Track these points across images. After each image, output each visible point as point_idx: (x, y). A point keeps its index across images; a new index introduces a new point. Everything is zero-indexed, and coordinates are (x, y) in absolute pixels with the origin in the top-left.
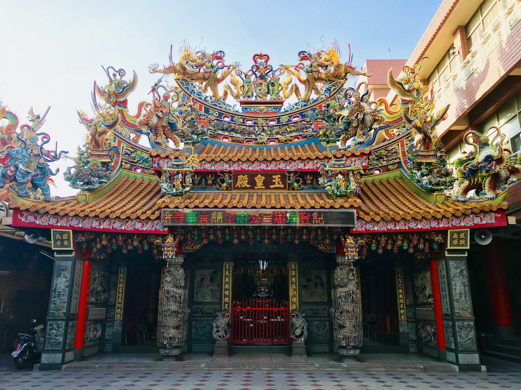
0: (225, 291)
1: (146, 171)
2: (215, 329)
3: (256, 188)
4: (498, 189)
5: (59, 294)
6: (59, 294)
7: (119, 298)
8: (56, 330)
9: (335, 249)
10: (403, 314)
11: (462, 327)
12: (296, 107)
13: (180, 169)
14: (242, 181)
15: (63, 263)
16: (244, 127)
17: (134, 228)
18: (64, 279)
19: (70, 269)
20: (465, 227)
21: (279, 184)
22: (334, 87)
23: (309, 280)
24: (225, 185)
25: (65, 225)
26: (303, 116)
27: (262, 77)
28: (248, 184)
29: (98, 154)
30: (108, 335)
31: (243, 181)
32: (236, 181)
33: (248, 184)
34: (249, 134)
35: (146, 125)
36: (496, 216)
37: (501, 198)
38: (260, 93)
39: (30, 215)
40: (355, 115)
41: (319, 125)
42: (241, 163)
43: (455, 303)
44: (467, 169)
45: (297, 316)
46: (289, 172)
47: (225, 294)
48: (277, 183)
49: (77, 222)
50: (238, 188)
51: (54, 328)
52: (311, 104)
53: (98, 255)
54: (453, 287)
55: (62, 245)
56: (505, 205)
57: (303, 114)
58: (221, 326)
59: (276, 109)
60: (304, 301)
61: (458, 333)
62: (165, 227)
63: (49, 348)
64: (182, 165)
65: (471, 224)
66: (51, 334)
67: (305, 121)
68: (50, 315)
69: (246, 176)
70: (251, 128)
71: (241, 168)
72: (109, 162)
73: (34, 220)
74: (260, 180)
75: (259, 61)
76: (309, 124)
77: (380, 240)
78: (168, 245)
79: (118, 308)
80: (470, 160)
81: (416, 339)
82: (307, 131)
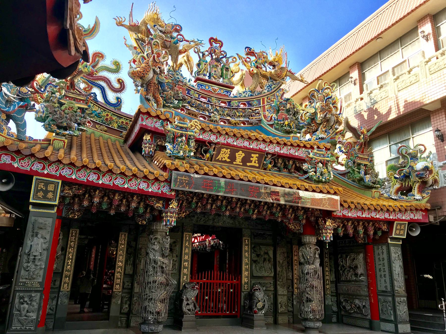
0: (184, 263)
1: (97, 126)
2: (185, 303)
3: (234, 163)
4: (424, 193)
5: (34, 259)
6: (34, 259)
7: (68, 265)
8: (27, 304)
9: (302, 229)
10: (328, 289)
11: (400, 302)
12: (243, 95)
13: (183, 132)
14: (224, 154)
15: (41, 220)
16: (199, 102)
17: (138, 188)
18: (42, 240)
19: (50, 228)
20: (405, 220)
21: (255, 162)
22: (274, 86)
23: (258, 256)
24: (208, 155)
25: (54, 173)
26: (250, 105)
27: (218, 60)
28: (228, 158)
29: (74, 96)
30: (50, 309)
31: (225, 154)
32: (219, 153)
33: (228, 158)
34: (204, 110)
35: (141, 78)
36: (422, 214)
37: (426, 200)
38: (215, 74)
39: (6, 154)
40: (325, 114)
41: (283, 116)
42: (227, 137)
43: (395, 282)
44: (402, 174)
45: (259, 289)
46: (268, 153)
47: (184, 265)
48: (253, 162)
49: (70, 171)
50: (218, 161)
51: (26, 302)
52: (256, 95)
53: (71, 214)
54: (394, 269)
55: (45, 198)
56: (428, 206)
57: (250, 103)
58: (191, 299)
59: (228, 92)
60: (254, 275)
61: (398, 307)
62: (172, 190)
63: (18, 328)
64: (186, 128)
65: (408, 218)
66: (22, 309)
67: (251, 109)
68: (20, 285)
69: (229, 150)
70: (205, 105)
71: (227, 141)
72: (86, 109)
73: (11, 162)
74: (240, 156)
75: (214, 45)
76: (255, 113)
77: (347, 225)
78: (172, 210)
79: (66, 277)
80: (402, 167)
81: (337, 311)
82: (252, 119)
